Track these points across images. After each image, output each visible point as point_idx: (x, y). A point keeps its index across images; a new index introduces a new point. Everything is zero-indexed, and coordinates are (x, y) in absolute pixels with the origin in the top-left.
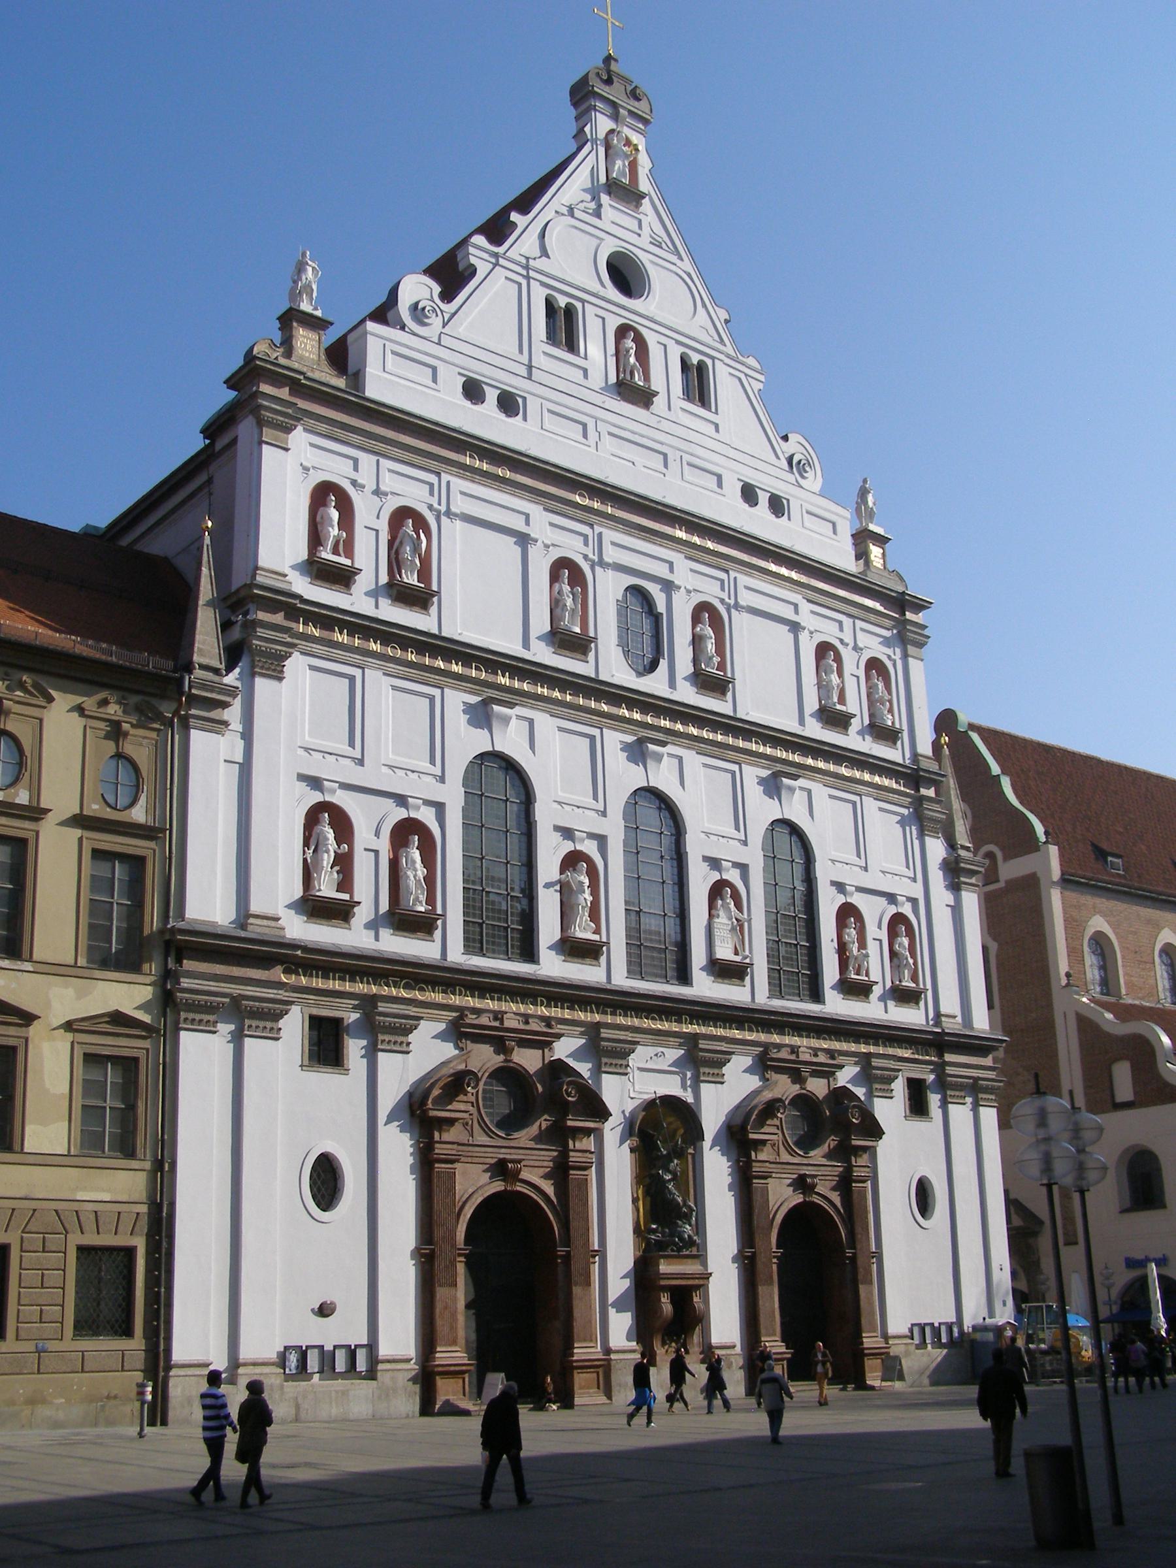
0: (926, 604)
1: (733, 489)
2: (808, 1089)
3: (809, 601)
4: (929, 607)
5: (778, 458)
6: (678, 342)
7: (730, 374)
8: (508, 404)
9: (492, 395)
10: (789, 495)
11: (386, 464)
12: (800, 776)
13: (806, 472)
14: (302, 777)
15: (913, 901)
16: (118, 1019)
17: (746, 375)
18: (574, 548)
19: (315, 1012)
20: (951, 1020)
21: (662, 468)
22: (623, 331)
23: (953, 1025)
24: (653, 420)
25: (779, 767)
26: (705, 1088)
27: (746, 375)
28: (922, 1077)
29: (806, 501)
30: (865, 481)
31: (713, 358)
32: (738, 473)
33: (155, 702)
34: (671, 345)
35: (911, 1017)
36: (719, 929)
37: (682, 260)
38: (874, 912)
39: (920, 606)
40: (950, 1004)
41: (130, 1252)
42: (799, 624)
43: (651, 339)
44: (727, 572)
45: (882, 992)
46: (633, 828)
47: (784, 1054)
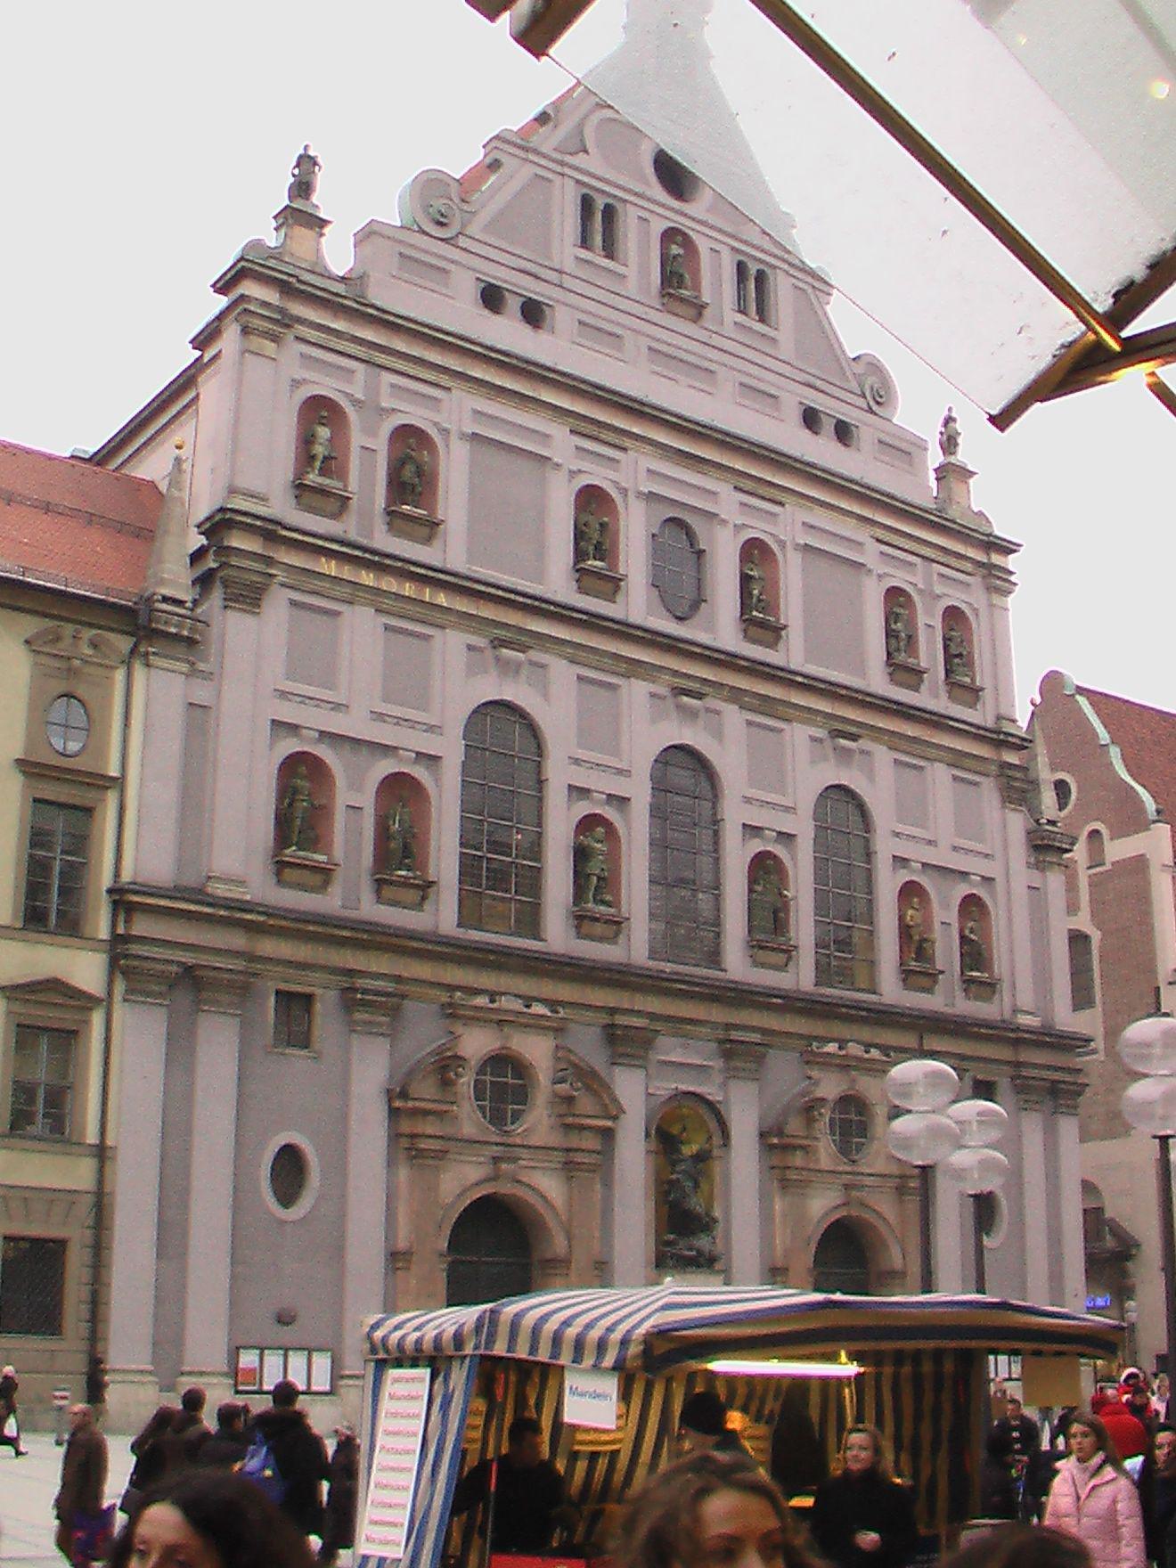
0: (1011, 546)
1: (795, 416)
3: (878, 540)
4: (1015, 551)
5: (848, 381)
8: (533, 313)
9: (513, 304)
12: (859, 736)
13: (881, 397)
15: (988, 880)
16: (54, 988)
19: (283, 986)
22: (670, 235)
24: (703, 336)
27: (814, 287)
30: (950, 409)
32: (798, 395)
33: (112, 636)
39: (1008, 549)
40: (1026, 998)
41: (61, 1244)
43: (703, 245)
46: (660, 787)
47: (831, 1048)
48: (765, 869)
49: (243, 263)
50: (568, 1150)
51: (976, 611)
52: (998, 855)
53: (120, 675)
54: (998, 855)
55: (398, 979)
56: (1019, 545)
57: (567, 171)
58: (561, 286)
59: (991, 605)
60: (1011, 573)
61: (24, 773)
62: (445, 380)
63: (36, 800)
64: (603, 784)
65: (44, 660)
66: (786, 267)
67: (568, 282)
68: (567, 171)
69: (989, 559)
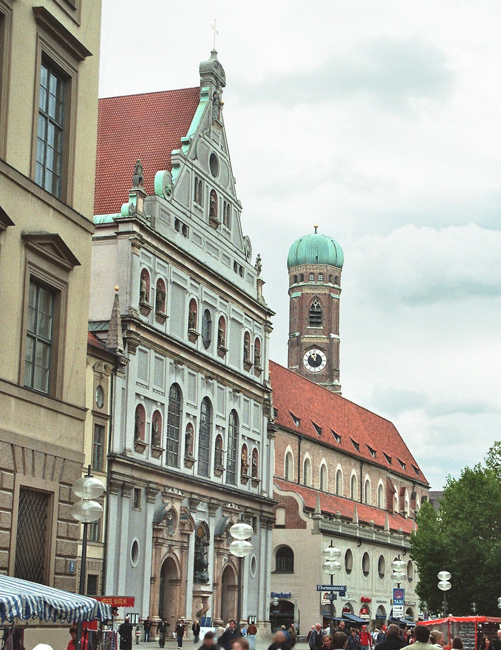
3: (245, 314)
4: (272, 315)
10: (245, 266)
11: (157, 260)
14: (136, 394)
17: (238, 210)
18: (194, 294)
23: (265, 495)
24: (216, 234)
25: (236, 388)
26: (211, 518)
27: (238, 210)
30: (259, 255)
31: (231, 203)
34: (222, 197)
35: (255, 491)
38: (251, 447)
40: (264, 488)
48: (219, 439)
49: (135, 219)
50: (181, 542)
51: (262, 339)
52: (261, 434)
53: (109, 378)
54: (261, 434)
55: (133, 478)
56: (275, 314)
57: (194, 169)
58: (190, 218)
59: (265, 337)
60: (272, 324)
61: (93, 415)
62: (168, 260)
63: (95, 424)
64: (193, 412)
65: (96, 374)
66: (233, 202)
67: (193, 217)
68: (194, 169)
69: (266, 318)
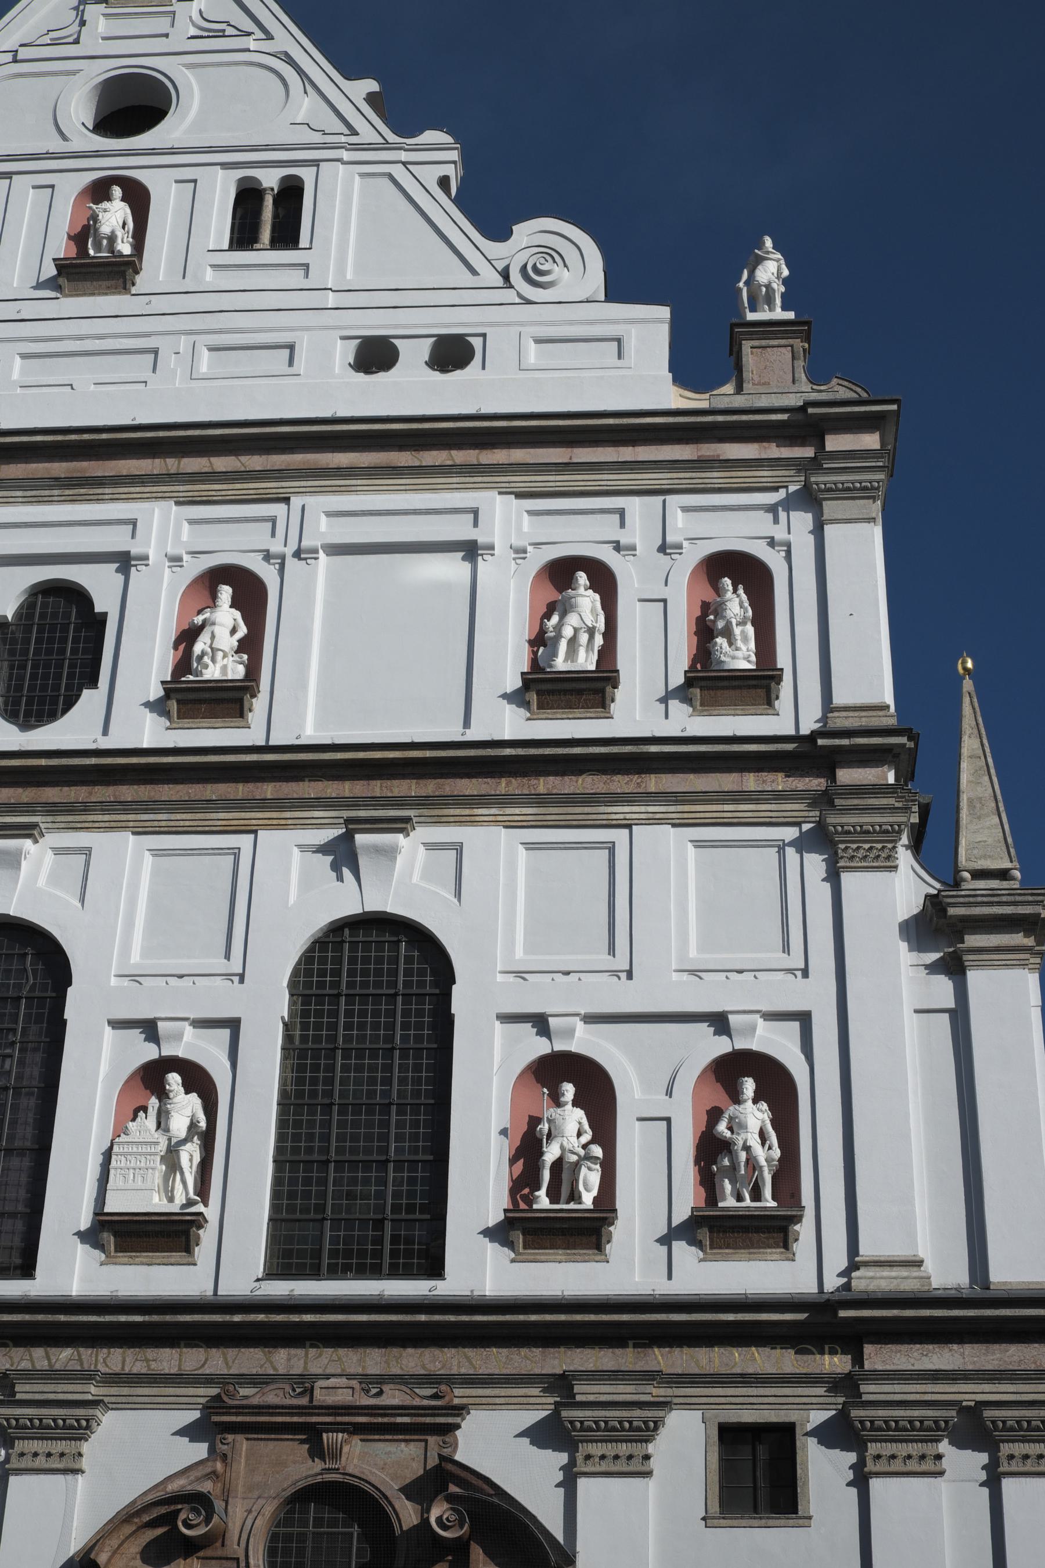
2: (350, 1470)
3: (519, 495)
5: (474, 272)
6: (225, 166)
7: (363, 175)
17: (404, 164)
20: (904, 1272)
21: (147, 374)
27: (404, 164)
28: (787, 1420)
29: (522, 324)
36: (124, 1154)
37: (270, 37)
42: (475, 542)
44: (286, 500)
45: (666, 1231)
